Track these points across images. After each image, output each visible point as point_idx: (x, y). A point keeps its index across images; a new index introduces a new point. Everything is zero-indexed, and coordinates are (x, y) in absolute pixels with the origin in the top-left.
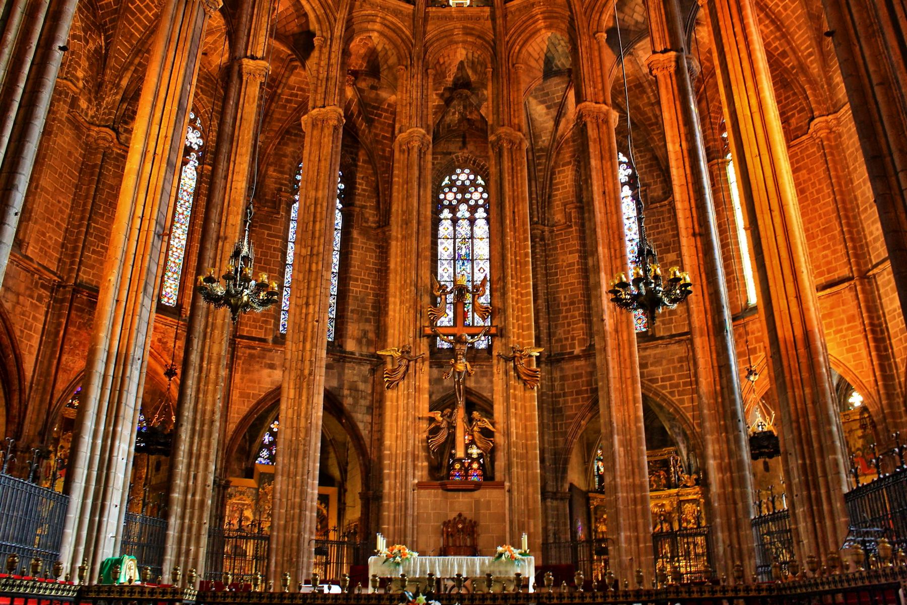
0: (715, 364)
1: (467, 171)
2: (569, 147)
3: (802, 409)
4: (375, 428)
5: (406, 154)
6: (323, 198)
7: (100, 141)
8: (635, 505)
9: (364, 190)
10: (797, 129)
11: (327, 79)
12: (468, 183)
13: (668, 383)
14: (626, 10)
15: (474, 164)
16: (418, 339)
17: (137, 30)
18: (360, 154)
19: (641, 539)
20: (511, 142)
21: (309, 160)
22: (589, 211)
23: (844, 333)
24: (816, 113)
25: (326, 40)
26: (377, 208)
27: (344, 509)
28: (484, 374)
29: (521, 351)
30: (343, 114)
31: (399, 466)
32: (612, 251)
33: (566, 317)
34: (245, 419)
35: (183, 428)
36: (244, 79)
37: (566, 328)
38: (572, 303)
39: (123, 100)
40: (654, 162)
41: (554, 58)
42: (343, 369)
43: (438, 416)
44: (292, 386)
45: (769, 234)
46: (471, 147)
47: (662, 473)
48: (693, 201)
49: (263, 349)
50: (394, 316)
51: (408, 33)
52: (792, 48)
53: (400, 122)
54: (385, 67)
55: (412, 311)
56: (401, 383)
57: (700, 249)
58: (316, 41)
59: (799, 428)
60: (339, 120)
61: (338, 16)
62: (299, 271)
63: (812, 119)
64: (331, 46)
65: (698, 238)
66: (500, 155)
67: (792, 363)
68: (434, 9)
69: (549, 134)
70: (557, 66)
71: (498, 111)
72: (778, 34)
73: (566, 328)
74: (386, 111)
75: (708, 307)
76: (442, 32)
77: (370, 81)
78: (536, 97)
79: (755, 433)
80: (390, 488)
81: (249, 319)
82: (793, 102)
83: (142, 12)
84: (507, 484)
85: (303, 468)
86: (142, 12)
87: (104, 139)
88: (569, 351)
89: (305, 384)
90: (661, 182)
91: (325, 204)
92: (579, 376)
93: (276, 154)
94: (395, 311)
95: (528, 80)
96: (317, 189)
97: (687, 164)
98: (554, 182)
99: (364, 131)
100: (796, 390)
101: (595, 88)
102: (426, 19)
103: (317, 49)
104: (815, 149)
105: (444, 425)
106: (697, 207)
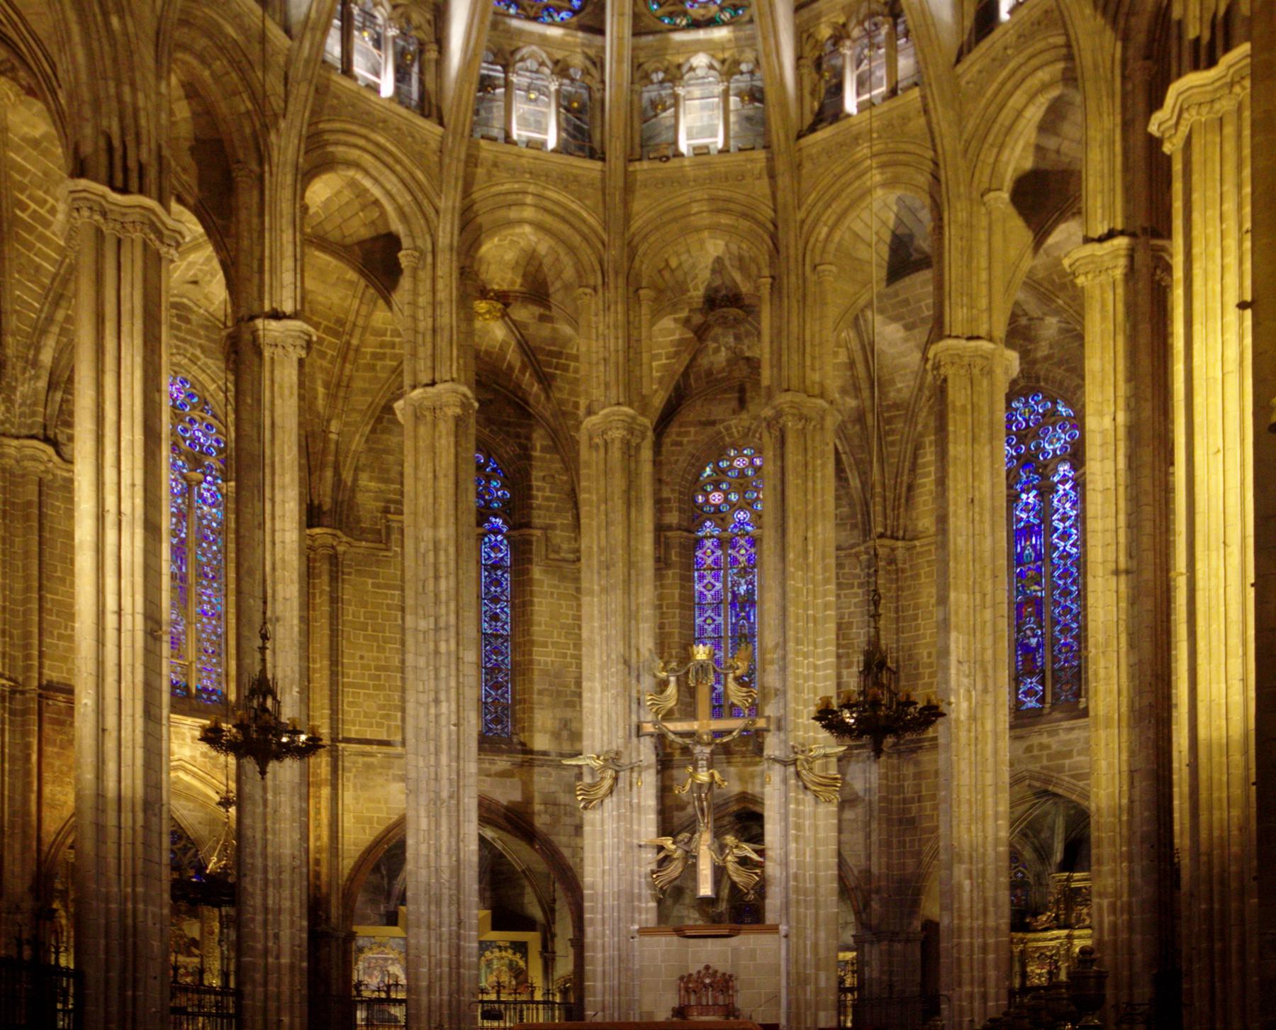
5: (602, 450)
21: (416, 479)
49: (388, 756)
51: (591, 220)
53: (587, 393)
58: (404, 258)
64: (434, 265)
68: (645, 165)
76: (665, 212)
78: (881, 311)
81: (357, 713)
102: (628, 189)
103: (407, 273)
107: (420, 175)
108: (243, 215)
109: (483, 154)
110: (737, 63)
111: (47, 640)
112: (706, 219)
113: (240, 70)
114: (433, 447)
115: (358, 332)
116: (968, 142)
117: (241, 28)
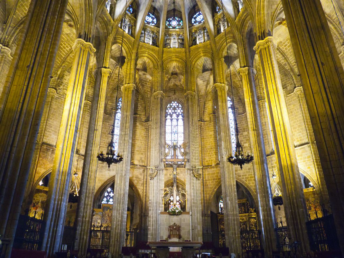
0: (261, 174)
1: (176, 102)
2: (210, 95)
3: (291, 193)
4: (145, 191)
5: (156, 100)
6: (129, 115)
7: (51, 93)
8: (234, 221)
10: (290, 90)
13: (244, 177)
14: (231, 50)
15: (178, 100)
16: (161, 163)
17: (63, 54)
18: (139, 96)
20: (192, 95)
21: (124, 102)
22: (218, 120)
23: (306, 162)
24: (297, 85)
25: (129, 60)
26: (145, 115)
27: (133, 219)
28: (181, 172)
29: (195, 167)
30: (135, 86)
31: (154, 206)
33: (209, 153)
34: (100, 188)
35: (82, 195)
37: (209, 157)
38: (211, 148)
39: (58, 78)
40: (240, 100)
41: (206, 65)
42: (134, 170)
43: (167, 189)
44: (118, 179)
45: (279, 133)
46: (177, 94)
47: (243, 207)
48: (253, 119)
50: (153, 155)
52: (288, 63)
53: (154, 88)
54: (149, 68)
55: (159, 153)
56: (155, 178)
58: (126, 60)
59: (290, 199)
60: (134, 88)
61: (133, 51)
62: (121, 140)
63: (295, 87)
64: (131, 62)
65: (255, 131)
66: (188, 100)
67: (287, 177)
68: (165, 49)
70: (207, 68)
71: (187, 85)
72: (283, 58)
73: (209, 157)
74: (148, 82)
77: (143, 72)
78: (199, 78)
79: (275, 197)
80: (151, 214)
82: (288, 81)
83: (65, 48)
84: (191, 213)
85: (122, 208)
86: (65, 48)
87: (52, 92)
88: (210, 165)
89: (123, 179)
90: (242, 107)
91: (130, 117)
92: (214, 174)
93: (111, 96)
94: (153, 153)
95: (197, 73)
96: (127, 112)
98: (205, 106)
99: (141, 89)
100: (289, 186)
101: (220, 78)
104: (296, 98)
105: (169, 192)
107: (130, 46)
108: (102, 49)
109: (140, 44)
110: (179, 34)
111: (45, 132)
112: (175, 59)
113: (106, 25)
114: (128, 96)
115: (113, 74)
116: (217, 50)
117: (107, 19)
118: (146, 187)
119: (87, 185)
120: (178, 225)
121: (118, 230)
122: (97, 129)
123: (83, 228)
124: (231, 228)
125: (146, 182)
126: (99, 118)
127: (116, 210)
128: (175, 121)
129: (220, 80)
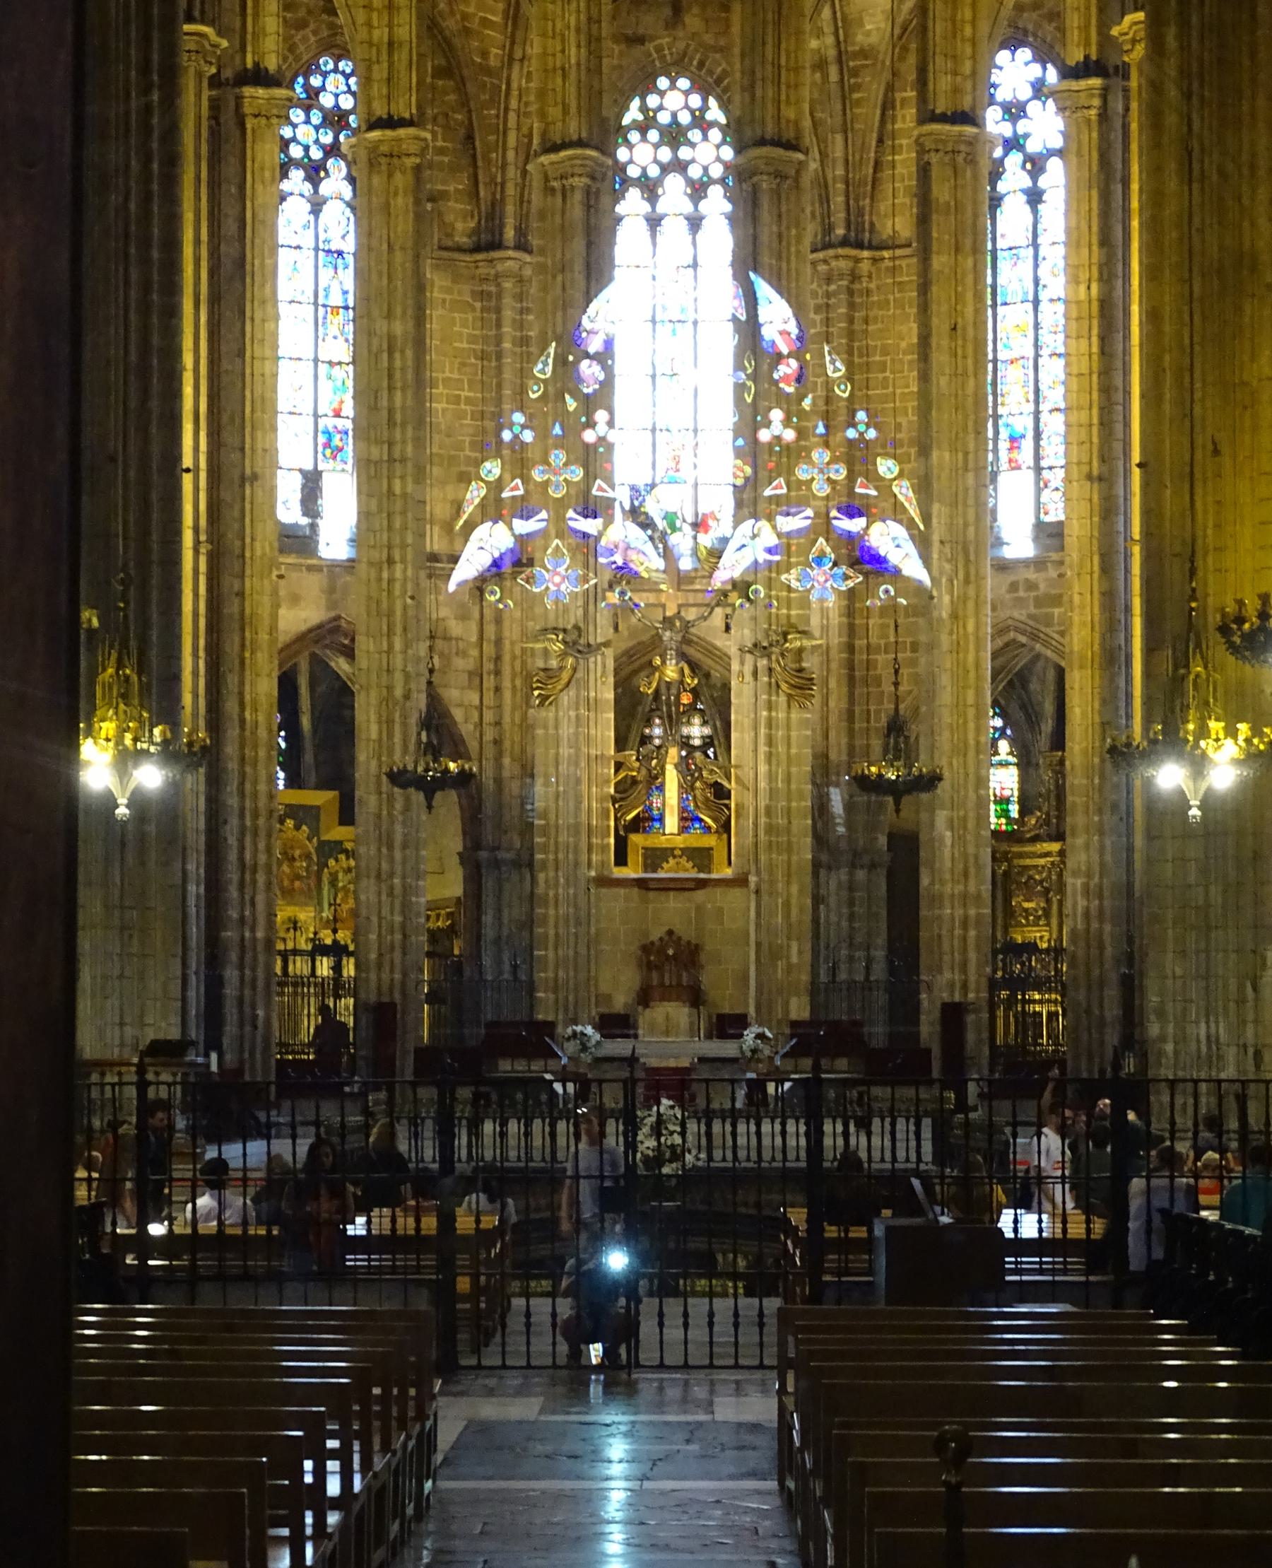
0: (1097, 719)
1: (683, 83)
4: (489, 716)
9: (441, 151)
11: (391, 44)
12: (685, 118)
15: (701, 64)
19: (972, 986)
20: (779, 175)
32: (960, 455)
36: (249, 126)
44: (373, 718)
46: (693, 21)
57: (1096, 508)
62: (369, 495)
65: (1096, 485)
69: (880, 17)
75: (1097, 619)
84: (753, 879)
89: (397, 715)
96: (389, 316)
97: (1095, 331)
106: (1101, 424)
118: (498, 689)
119: (243, 775)
120: (685, 938)
121: (392, 971)
122: (258, 470)
123: (247, 972)
124: (946, 958)
125: (498, 659)
126: (258, 405)
127: (373, 874)
128: (675, 228)
129: (956, 90)
